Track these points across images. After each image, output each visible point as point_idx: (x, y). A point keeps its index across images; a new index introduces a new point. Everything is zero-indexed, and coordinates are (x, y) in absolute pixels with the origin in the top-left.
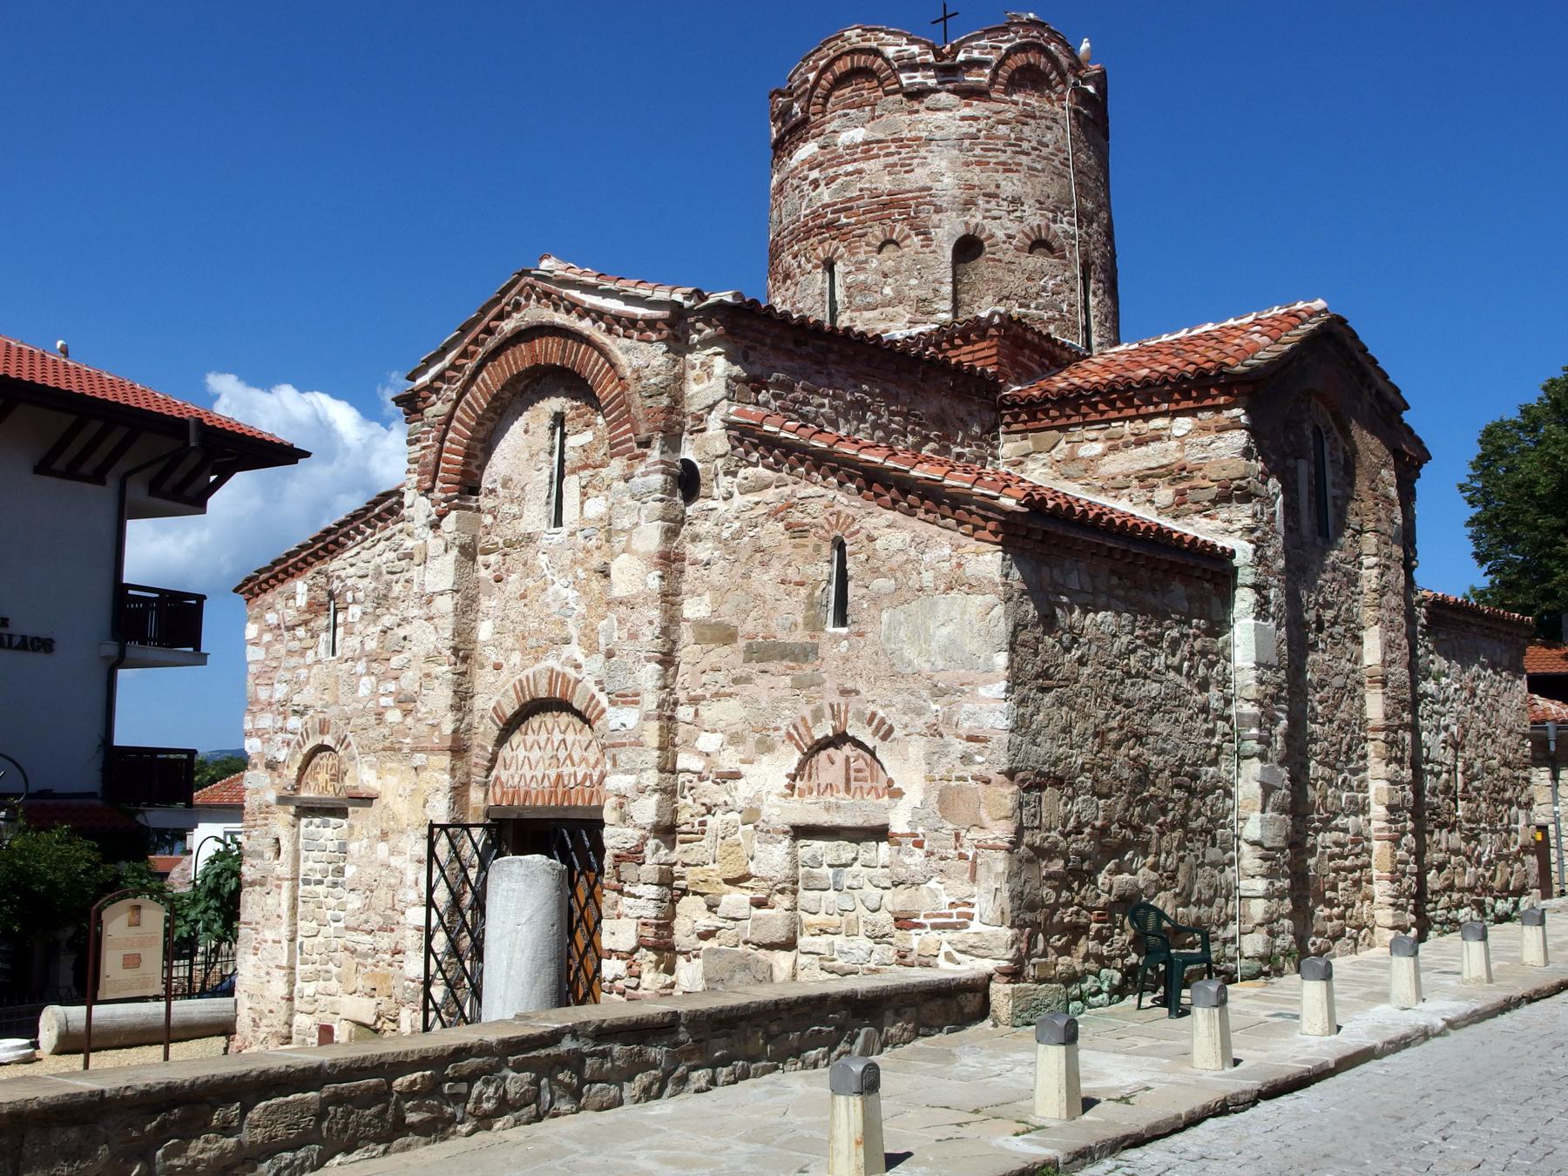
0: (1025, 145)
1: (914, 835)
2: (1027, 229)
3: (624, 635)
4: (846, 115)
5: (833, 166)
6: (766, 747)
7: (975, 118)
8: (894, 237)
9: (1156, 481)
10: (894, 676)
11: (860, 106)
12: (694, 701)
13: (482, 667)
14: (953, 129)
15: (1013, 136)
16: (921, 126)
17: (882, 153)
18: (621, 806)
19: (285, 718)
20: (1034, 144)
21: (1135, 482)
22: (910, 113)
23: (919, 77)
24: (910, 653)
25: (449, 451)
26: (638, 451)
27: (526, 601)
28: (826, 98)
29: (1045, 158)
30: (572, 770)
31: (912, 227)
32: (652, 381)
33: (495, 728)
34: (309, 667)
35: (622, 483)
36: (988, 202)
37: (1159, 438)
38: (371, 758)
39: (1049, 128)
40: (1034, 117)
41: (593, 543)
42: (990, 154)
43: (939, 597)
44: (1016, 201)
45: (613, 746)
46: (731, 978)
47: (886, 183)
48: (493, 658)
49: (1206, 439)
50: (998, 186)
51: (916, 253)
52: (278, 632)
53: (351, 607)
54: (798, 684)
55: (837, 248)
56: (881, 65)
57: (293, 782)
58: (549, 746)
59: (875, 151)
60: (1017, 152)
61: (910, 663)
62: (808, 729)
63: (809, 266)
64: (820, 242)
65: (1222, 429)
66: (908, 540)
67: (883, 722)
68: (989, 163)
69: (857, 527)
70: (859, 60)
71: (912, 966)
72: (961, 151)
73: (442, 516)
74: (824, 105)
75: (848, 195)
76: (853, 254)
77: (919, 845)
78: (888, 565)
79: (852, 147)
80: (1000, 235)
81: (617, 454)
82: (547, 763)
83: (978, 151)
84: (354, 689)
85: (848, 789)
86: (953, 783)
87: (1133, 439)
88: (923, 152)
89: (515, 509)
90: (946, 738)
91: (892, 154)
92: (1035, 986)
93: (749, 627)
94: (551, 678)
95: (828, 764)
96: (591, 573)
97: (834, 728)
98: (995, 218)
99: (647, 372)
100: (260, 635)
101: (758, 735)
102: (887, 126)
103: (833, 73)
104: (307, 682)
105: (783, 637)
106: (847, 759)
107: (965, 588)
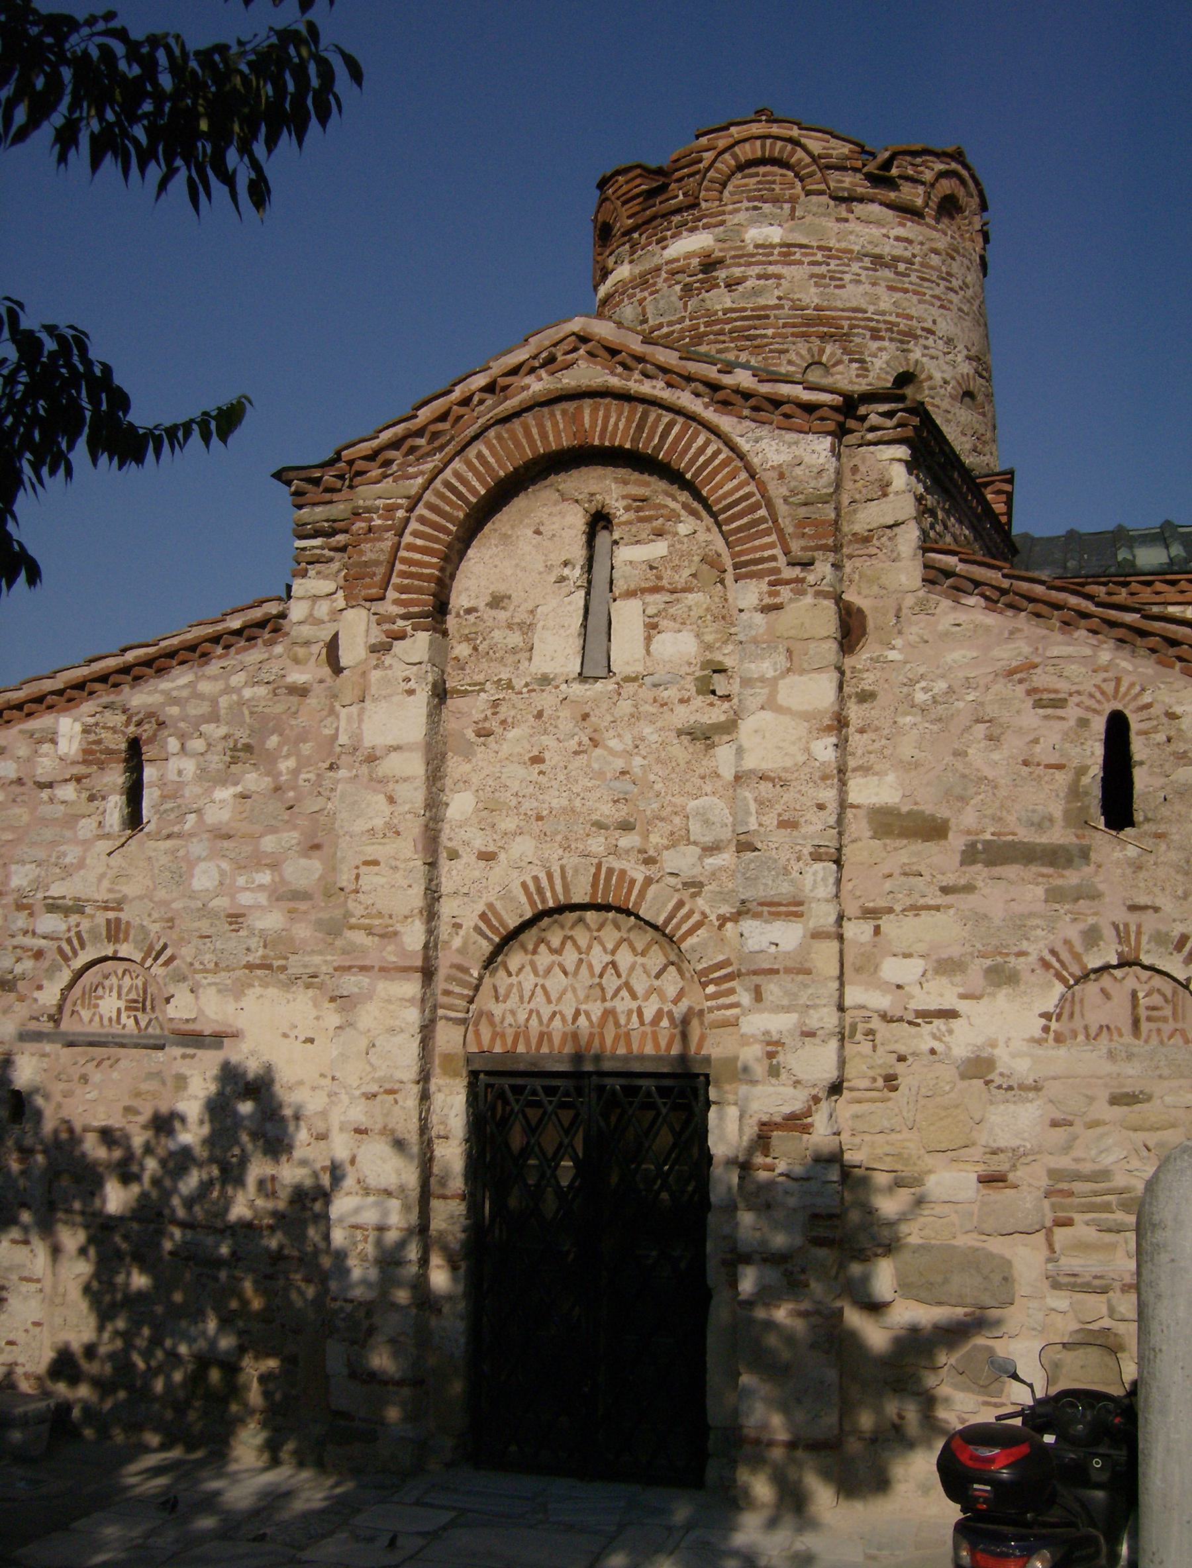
0: (955, 283)
3: (771, 820)
4: (755, 208)
5: (740, 265)
7: (909, 241)
8: (824, 360)
11: (776, 201)
12: (870, 914)
13: (454, 855)
15: (944, 269)
16: (852, 238)
18: (771, 1055)
22: (839, 220)
23: (848, 181)
25: (411, 547)
27: (542, 767)
28: (724, 185)
30: (634, 1005)
31: (846, 351)
33: (485, 943)
36: (927, 338)
40: (958, 252)
42: (926, 284)
44: (949, 341)
45: (755, 973)
46: (946, 1281)
47: (811, 296)
50: (934, 322)
52: (17, 789)
54: (1055, 895)
56: (800, 160)
57: (53, 1011)
58: (584, 969)
60: (948, 289)
62: (1077, 957)
68: (925, 294)
69: (1147, 698)
70: (773, 146)
72: (897, 273)
74: (721, 193)
75: (762, 301)
79: (767, 247)
80: (938, 376)
82: (581, 994)
88: (855, 267)
89: (515, 639)
91: (818, 264)
94: (596, 876)
95: (1099, 998)
96: (674, 734)
97: (1120, 955)
98: (932, 358)
99: (798, 471)
103: (735, 156)
104: (81, 865)
105: (1026, 835)
106: (1134, 994)
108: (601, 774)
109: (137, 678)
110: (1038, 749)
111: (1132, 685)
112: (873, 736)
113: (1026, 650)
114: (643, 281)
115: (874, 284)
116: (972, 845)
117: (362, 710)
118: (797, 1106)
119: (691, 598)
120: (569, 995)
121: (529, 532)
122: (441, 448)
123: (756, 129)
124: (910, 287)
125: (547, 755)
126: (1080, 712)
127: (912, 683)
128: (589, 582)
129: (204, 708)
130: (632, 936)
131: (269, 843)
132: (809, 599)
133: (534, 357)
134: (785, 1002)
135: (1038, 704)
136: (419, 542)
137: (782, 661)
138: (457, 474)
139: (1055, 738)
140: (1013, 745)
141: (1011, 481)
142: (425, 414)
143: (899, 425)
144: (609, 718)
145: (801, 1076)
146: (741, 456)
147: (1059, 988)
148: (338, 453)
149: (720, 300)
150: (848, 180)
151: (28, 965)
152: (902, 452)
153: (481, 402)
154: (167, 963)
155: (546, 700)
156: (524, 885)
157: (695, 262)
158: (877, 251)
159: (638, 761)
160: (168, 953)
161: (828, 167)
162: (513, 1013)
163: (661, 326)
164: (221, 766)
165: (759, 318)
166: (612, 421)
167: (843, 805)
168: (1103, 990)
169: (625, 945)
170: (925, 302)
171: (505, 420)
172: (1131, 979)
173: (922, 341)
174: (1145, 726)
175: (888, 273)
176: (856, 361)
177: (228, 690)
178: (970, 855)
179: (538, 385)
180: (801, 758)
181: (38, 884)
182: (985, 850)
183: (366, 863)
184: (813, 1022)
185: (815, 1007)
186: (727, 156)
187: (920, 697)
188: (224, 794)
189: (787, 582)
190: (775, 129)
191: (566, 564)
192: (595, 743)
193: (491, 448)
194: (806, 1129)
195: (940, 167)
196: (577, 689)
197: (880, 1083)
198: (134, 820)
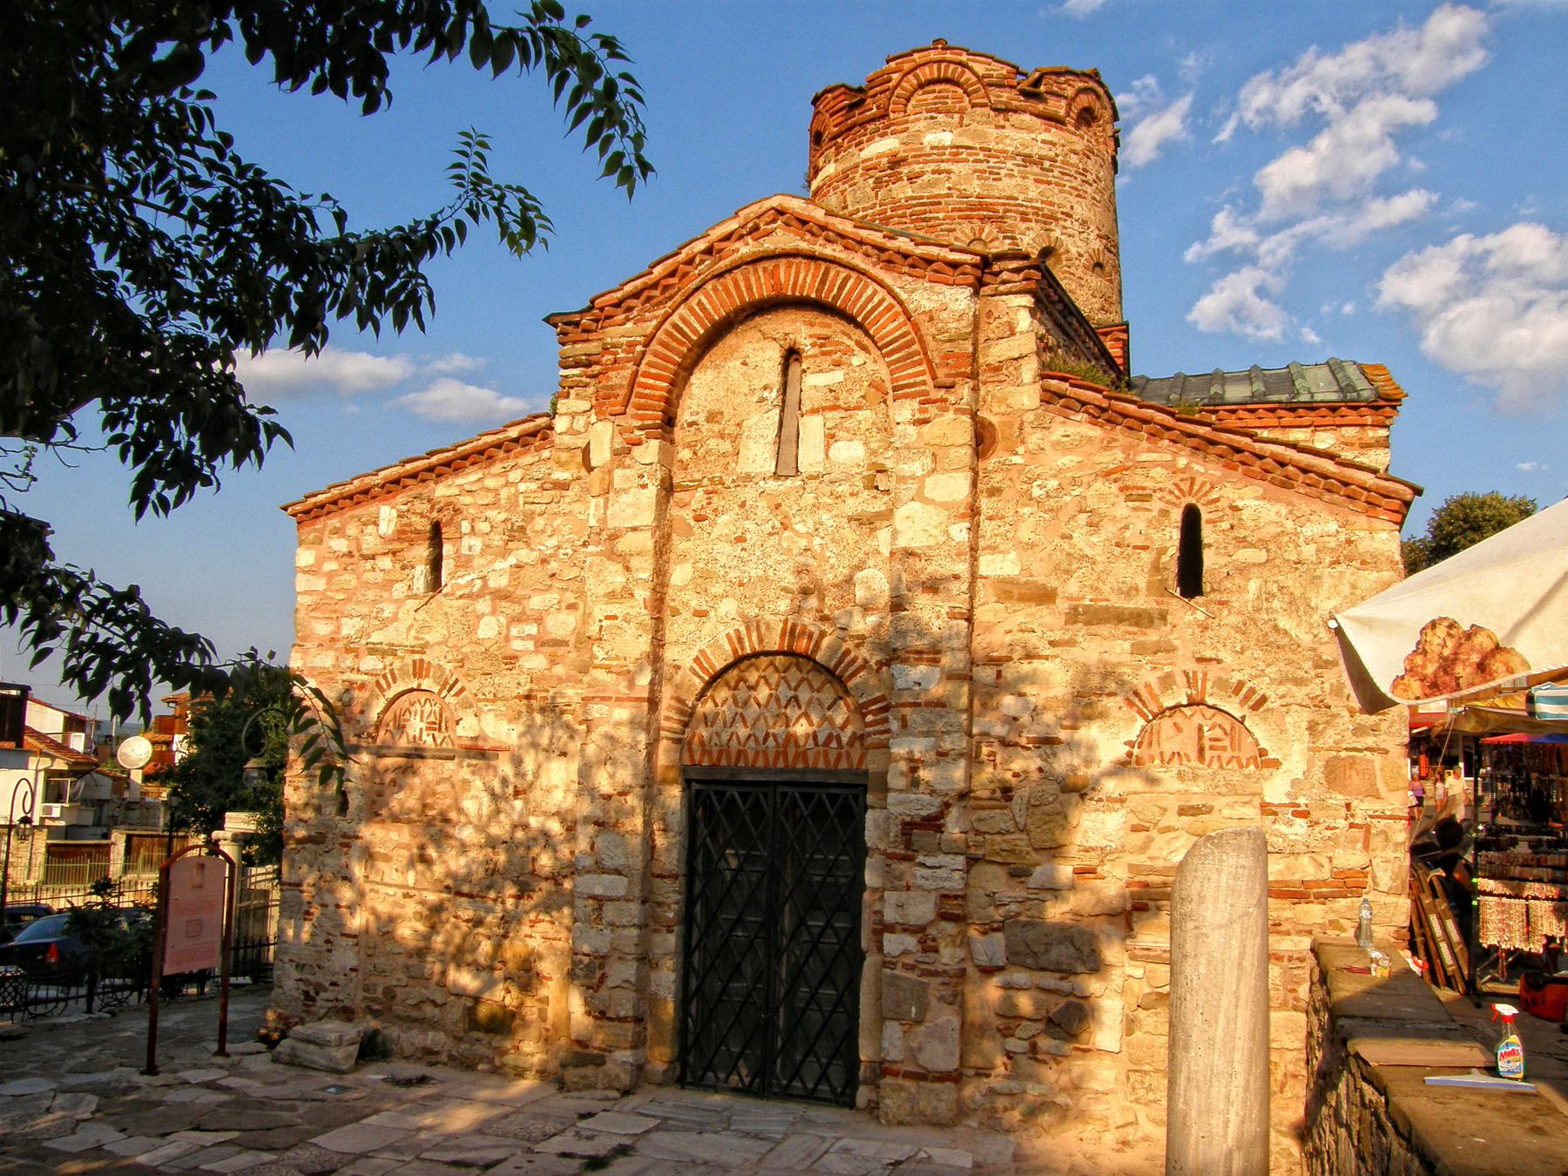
0: (1090, 178)
7: (1054, 144)
10: (1266, 645)
11: (948, 112)
13: (676, 612)
14: (1035, 150)
22: (997, 127)
23: (1005, 96)
24: (1283, 623)
25: (646, 375)
28: (908, 100)
31: (1000, 230)
33: (697, 681)
35: (911, 430)
38: (500, 705)
43: (1324, 571)
44: (1084, 223)
46: (1047, 951)
47: (975, 187)
48: (694, 603)
52: (349, 560)
61: (1286, 633)
62: (1154, 697)
67: (1252, 691)
69: (1214, 495)
70: (947, 68)
71: (1288, 933)
75: (936, 191)
77: (1304, 814)
78: (1257, 535)
80: (1074, 250)
81: (906, 396)
83: (1056, 173)
84: (471, 630)
86: (1343, 754)
88: (1010, 164)
90: (1334, 710)
93: (1072, 587)
95: (1172, 731)
97: (1189, 697)
99: (944, 315)
102: (977, 135)
103: (917, 77)
104: (395, 618)
105: (1118, 602)
107: (1356, 564)
108: (789, 551)
109: (439, 475)
110: (1128, 534)
111: (1204, 484)
112: (999, 522)
113: (1120, 456)
114: (845, 176)
116: (1075, 608)
117: (607, 500)
118: (932, 810)
119: (861, 415)
120: (762, 721)
121: (738, 363)
122: (671, 298)
123: (933, 55)
125: (748, 536)
126: (1162, 505)
127: (1030, 481)
128: (784, 401)
129: (490, 498)
130: (810, 676)
131: (536, 602)
132: (950, 415)
133: (743, 227)
135: (1129, 498)
136: (653, 371)
137: (928, 461)
138: (683, 319)
139: (1141, 525)
140: (1108, 530)
141: (1126, 331)
142: (658, 271)
143: (1025, 279)
144: (796, 507)
146: (901, 303)
147: (1141, 722)
148: (592, 302)
149: (903, 191)
153: (702, 262)
154: (457, 694)
155: (749, 494)
156: (728, 636)
157: (885, 160)
158: (1027, 151)
159: (817, 541)
160: (458, 686)
161: (990, 85)
162: (718, 735)
163: (857, 211)
166: (802, 276)
167: (974, 576)
169: (805, 684)
171: (720, 275)
172: (1197, 717)
174: (1213, 516)
175: (1036, 169)
177: (507, 484)
178: (1073, 616)
179: (745, 249)
180: (942, 539)
181: (364, 633)
182: (1084, 613)
183: (608, 618)
184: (947, 745)
185: (948, 733)
186: (910, 77)
187: (1036, 492)
188: (504, 565)
189: (934, 402)
190: (949, 55)
191: (765, 388)
194: (939, 829)
195: (1081, 85)
196: (772, 485)
197: (998, 794)
198: (435, 584)
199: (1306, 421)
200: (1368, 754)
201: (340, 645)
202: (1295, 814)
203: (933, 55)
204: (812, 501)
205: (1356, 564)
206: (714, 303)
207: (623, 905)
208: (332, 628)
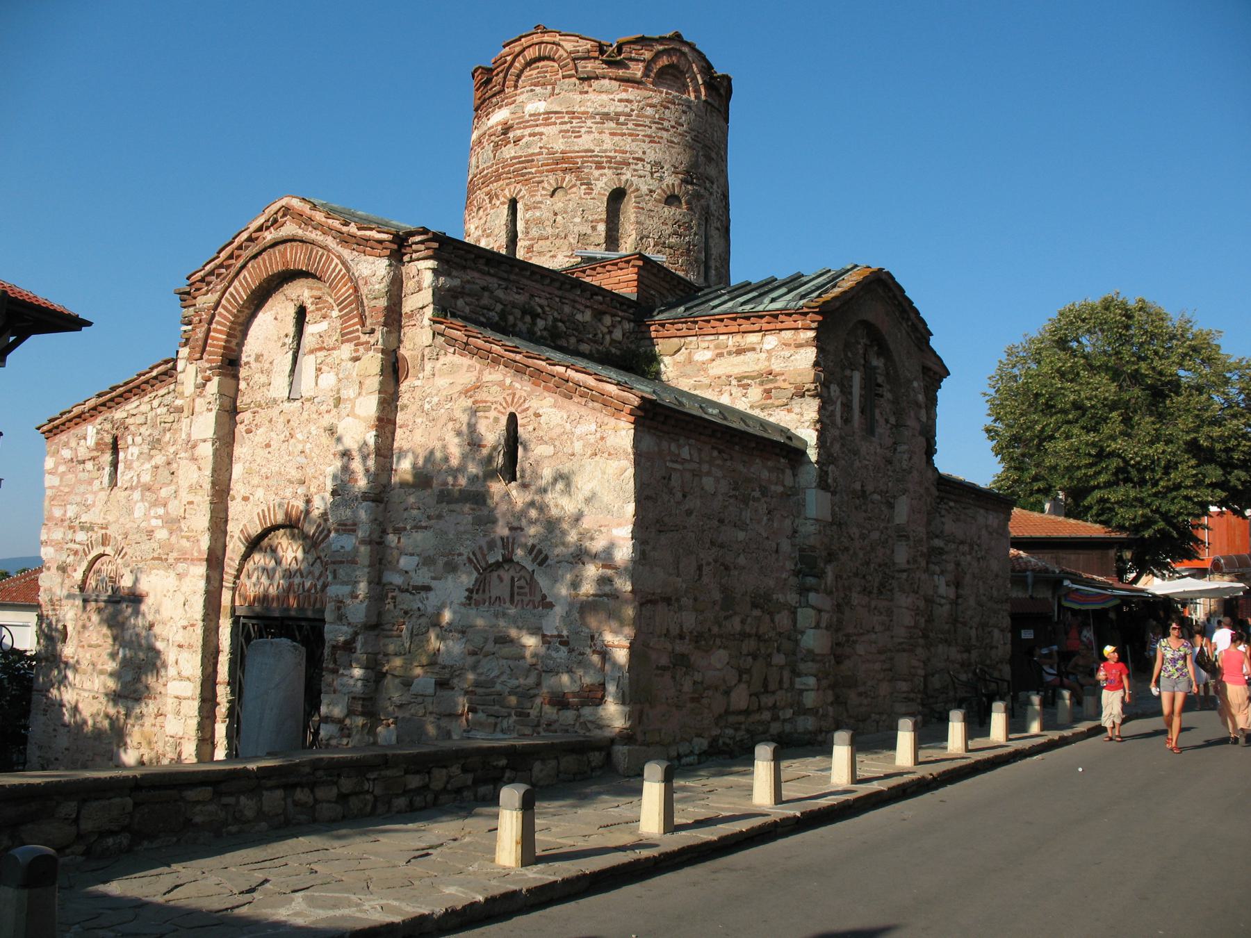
0: (666, 124)
1: (560, 636)
2: (664, 186)
4: (532, 90)
5: (520, 128)
6: (452, 568)
7: (628, 101)
9: (749, 382)
14: (612, 109)
15: (657, 116)
17: (558, 121)
18: (339, 608)
19: (74, 532)
20: (673, 123)
21: (734, 382)
22: (581, 93)
23: (590, 66)
26: (364, 338)
27: (269, 449)
28: (519, 76)
29: (680, 134)
31: (578, 178)
32: (377, 287)
33: (242, 546)
34: (95, 493)
35: (350, 363)
36: (636, 164)
37: (754, 349)
39: (684, 112)
40: (674, 103)
41: (324, 408)
42: (640, 128)
47: (559, 145)
49: (787, 354)
51: (581, 198)
52: (71, 465)
53: (130, 448)
55: (521, 190)
59: (553, 120)
60: (660, 129)
62: (484, 556)
63: (498, 203)
64: (507, 185)
65: (799, 346)
66: (565, 417)
69: (526, 405)
70: (545, 50)
72: (617, 124)
73: (209, 379)
75: (530, 151)
76: (533, 196)
77: (565, 643)
81: (348, 341)
83: (630, 125)
84: (130, 512)
85: (512, 601)
87: (734, 349)
88: (589, 123)
91: (566, 123)
92: (644, 748)
96: (322, 430)
99: (374, 279)
100: (56, 466)
101: (446, 559)
103: (524, 58)
104: (94, 505)
106: (513, 579)
107: (606, 455)
115: (600, 133)
123: (536, 39)
124: (627, 132)
125: (272, 443)
132: (371, 353)
133: (268, 220)
134: (346, 580)
136: (219, 327)
142: (223, 255)
143: (427, 248)
145: (351, 620)
147: (475, 575)
150: (589, 65)
151: (72, 558)
152: (431, 263)
155: (274, 413)
157: (499, 128)
158: (606, 110)
159: (308, 445)
161: (578, 59)
163: (484, 170)
164: (147, 451)
165: (528, 161)
168: (499, 576)
170: (637, 141)
171: (255, 257)
173: (633, 167)
174: (524, 421)
175: (612, 125)
176: (584, 184)
179: (269, 236)
187: (427, 406)
190: (546, 38)
191: (287, 336)
192: (292, 436)
193: (250, 273)
195: (661, 48)
196: (286, 404)
199: (757, 327)
200: (606, 599)
201: (66, 524)
202: (562, 643)
203: (536, 39)
204: (307, 417)
205: (606, 455)
206: (251, 277)
207: (190, 702)
208: (62, 512)
